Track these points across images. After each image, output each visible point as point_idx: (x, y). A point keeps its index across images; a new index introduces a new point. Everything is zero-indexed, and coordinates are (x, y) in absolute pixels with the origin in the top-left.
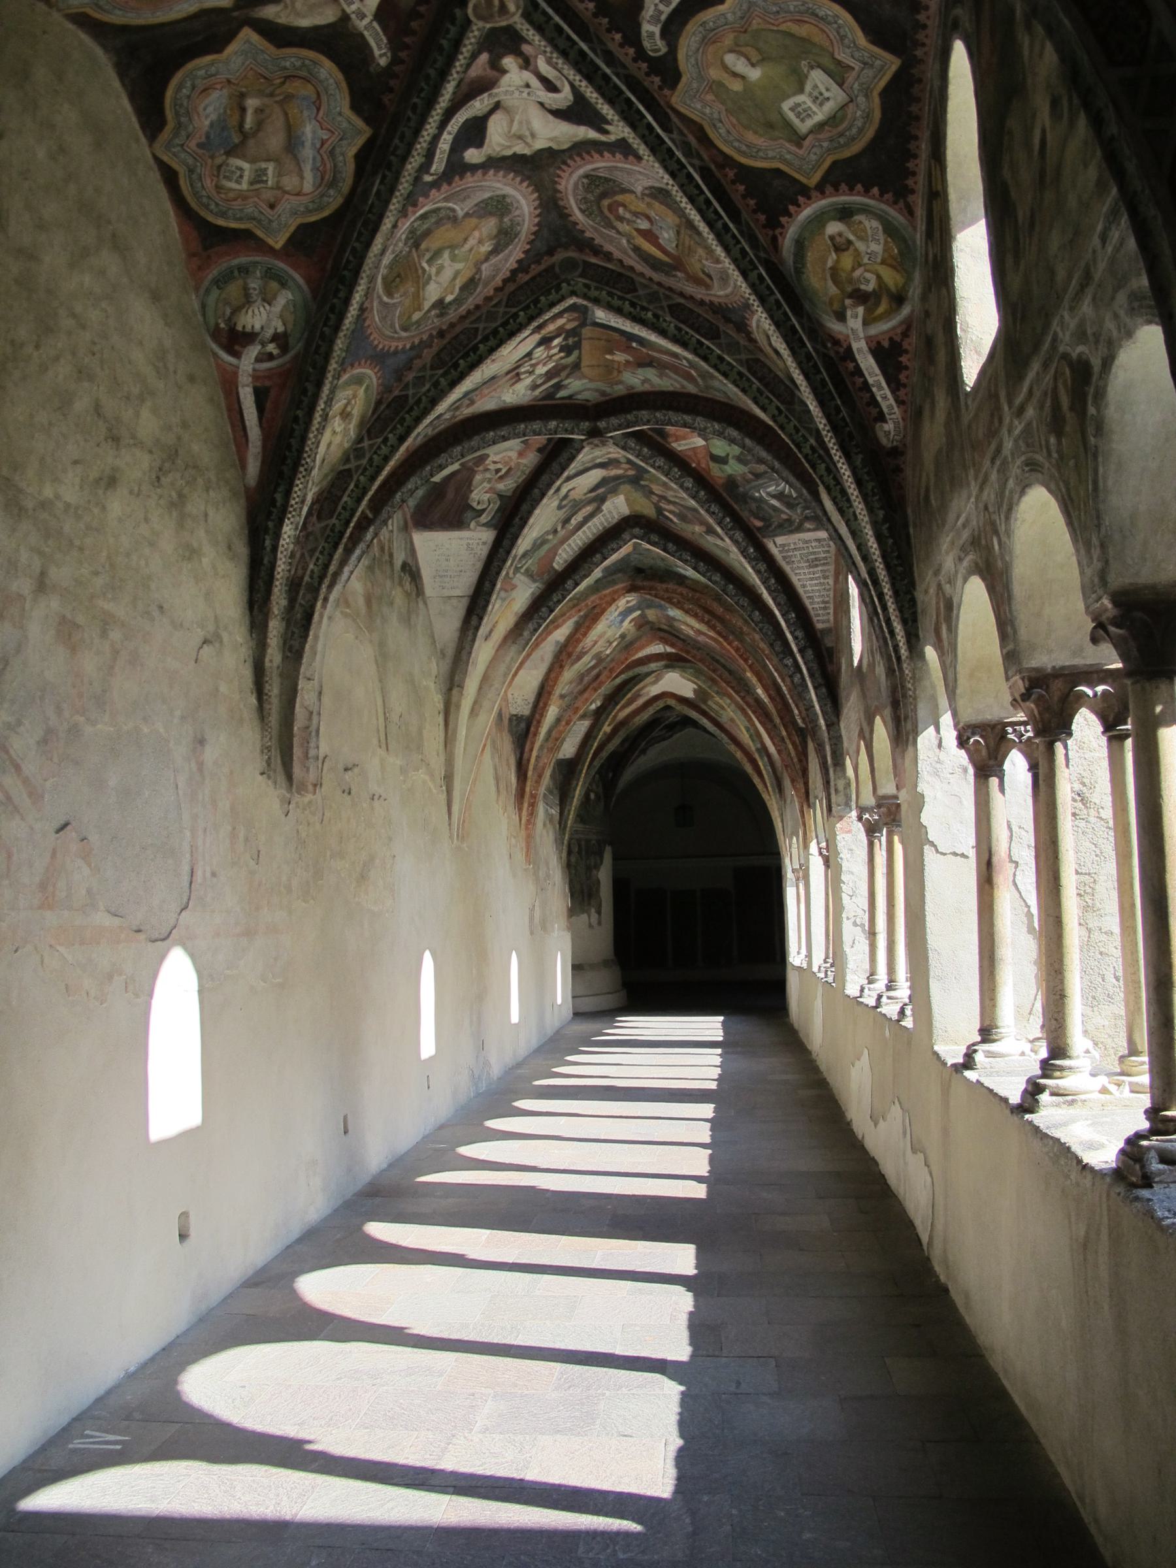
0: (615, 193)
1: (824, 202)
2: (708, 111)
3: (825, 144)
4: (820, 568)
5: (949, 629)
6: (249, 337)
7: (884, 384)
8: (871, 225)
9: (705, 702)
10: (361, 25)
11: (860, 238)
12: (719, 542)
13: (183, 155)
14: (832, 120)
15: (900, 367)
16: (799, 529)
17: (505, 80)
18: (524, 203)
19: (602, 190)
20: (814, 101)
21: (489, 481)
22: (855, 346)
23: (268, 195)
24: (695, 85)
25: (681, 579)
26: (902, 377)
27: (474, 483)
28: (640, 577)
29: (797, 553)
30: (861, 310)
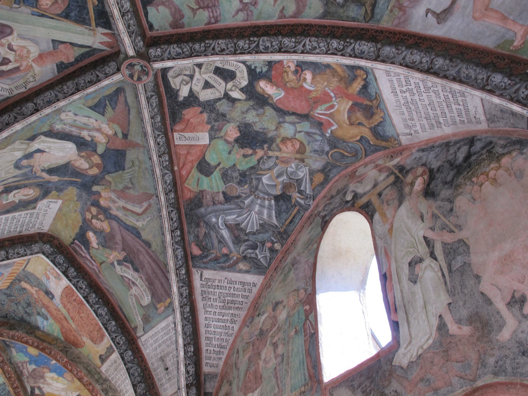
4: (231, 312)
16: (232, 268)
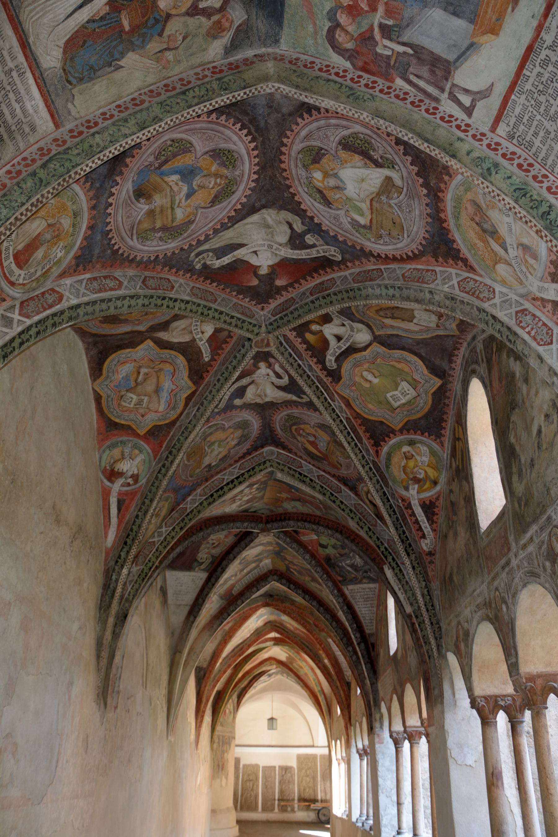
0: (300, 424)
1: (402, 437)
2: (352, 394)
3: (405, 413)
5: (467, 646)
6: (120, 474)
7: (426, 521)
8: (424, 449)
9: (292, 663)
10: (200, 344)
11: (418, 454)
12: (318, 586)
13: (106, 390)
14: (409, 403)
15: (434, 514)
16: (360, 582)
17: (259, 371)
18: (255, 423)
19: (293, 422)
20: (402, 394)
21: (208, 548)
22: (412, 503)
23: (142, 411)
24: (348, 382)
25: (293, 602)
26: (435, 518)
27: (201, 548)
28: (272, 600)
29: (359, 594)
30: (416, 486)
